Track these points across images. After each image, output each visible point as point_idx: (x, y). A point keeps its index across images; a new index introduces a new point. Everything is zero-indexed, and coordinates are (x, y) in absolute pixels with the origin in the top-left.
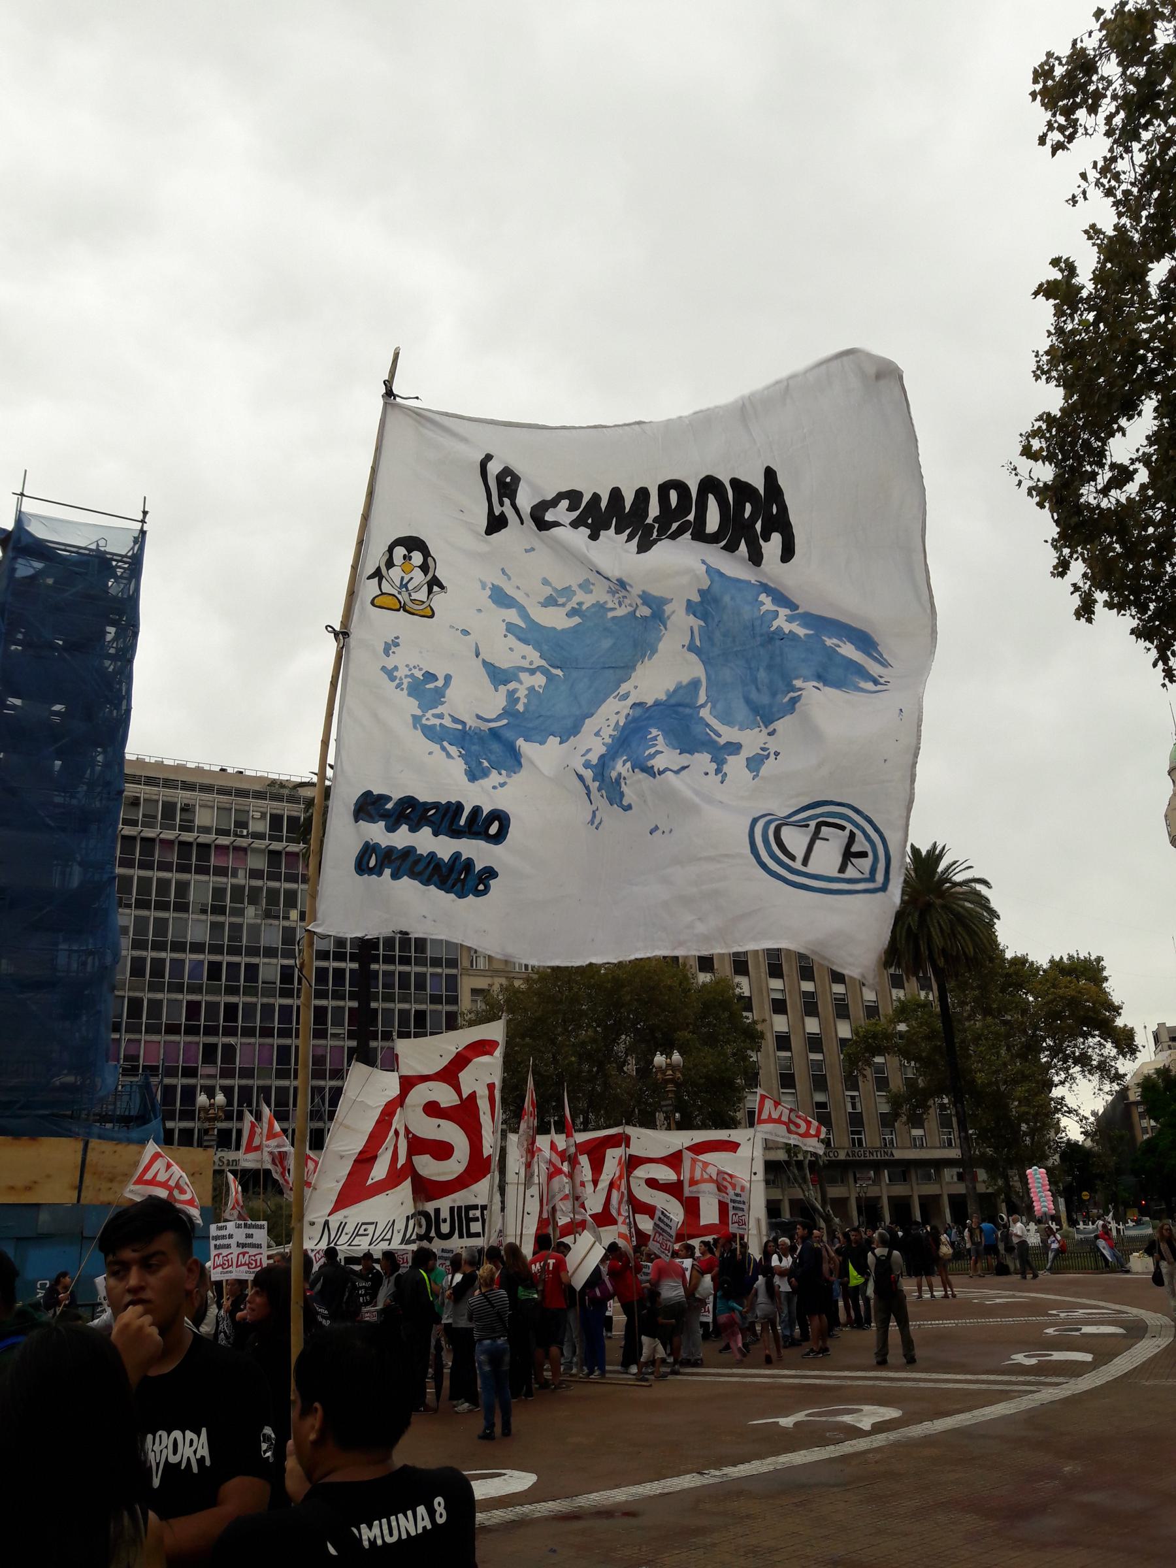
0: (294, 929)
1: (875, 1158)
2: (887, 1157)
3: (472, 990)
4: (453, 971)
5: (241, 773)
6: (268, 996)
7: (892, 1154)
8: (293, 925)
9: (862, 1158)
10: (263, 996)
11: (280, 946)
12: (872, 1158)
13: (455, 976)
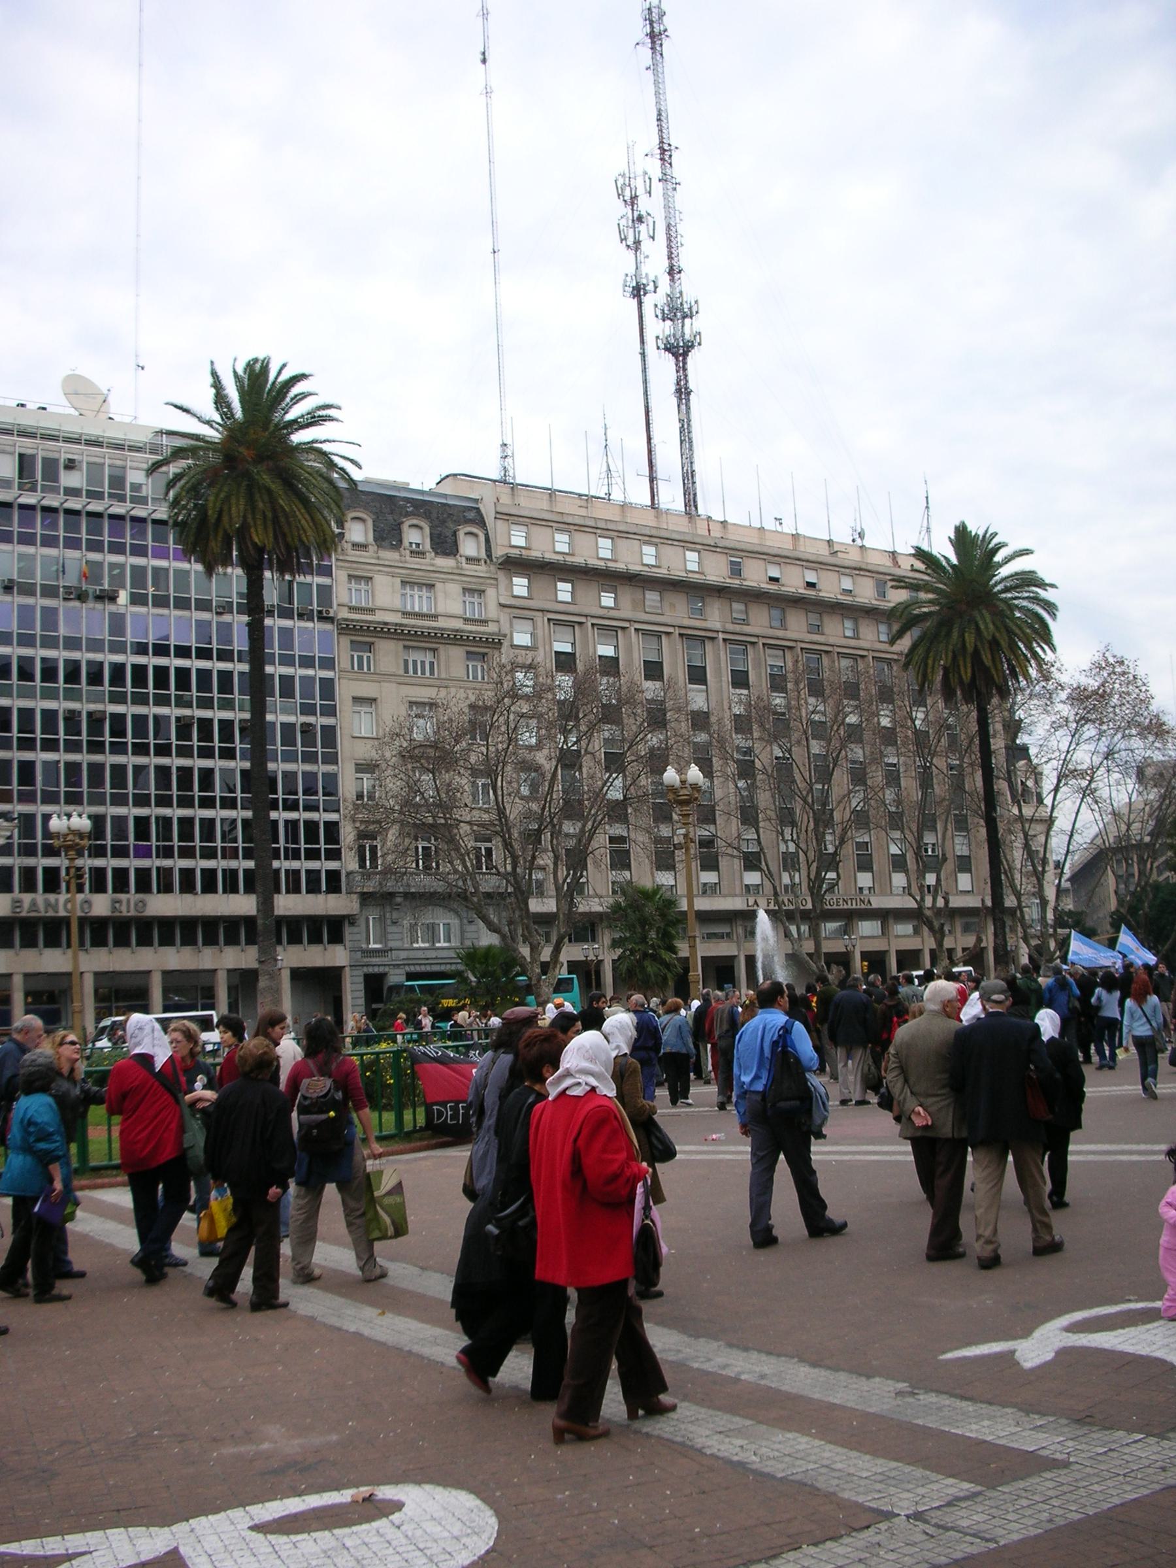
0: (123, 616)
1: (849, 906)
2: (863, 906)
3: (354, 698)
4: (328, 674)
5: (44, 409)
6: (95, 702)
7: (869, 902)
8: (122, 610)
9: (835, 907)
10: (88, 701)
11: (108, 638)
12: (846, 907)
13: (331, 680)
